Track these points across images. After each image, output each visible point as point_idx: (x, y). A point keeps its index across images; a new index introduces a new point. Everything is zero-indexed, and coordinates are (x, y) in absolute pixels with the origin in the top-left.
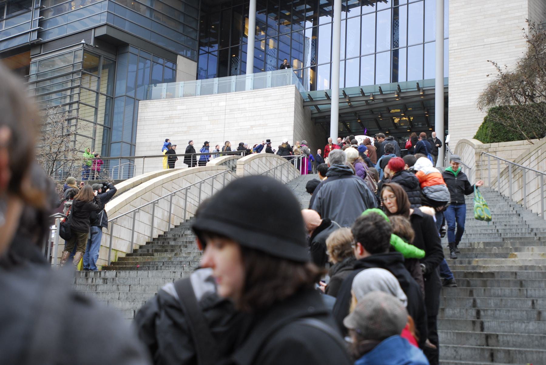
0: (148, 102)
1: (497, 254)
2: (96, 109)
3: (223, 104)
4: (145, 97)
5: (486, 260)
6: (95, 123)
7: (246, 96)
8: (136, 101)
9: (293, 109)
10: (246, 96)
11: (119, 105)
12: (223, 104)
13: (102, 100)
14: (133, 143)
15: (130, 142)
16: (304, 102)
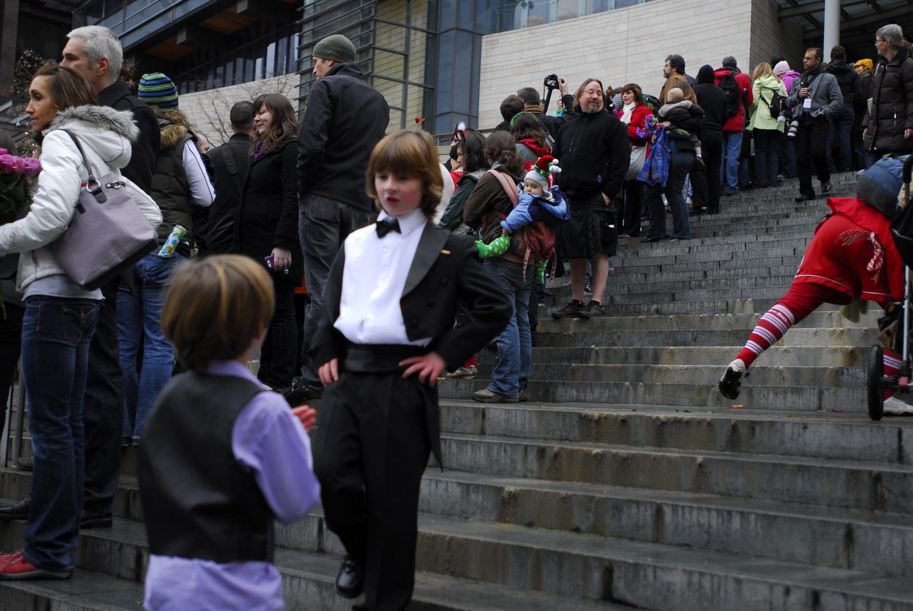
0: (496, 36)
1: (737, 332)
2: (406, 57)
3: (623, 27)
4: (498, 26)
5: (691, 350)
6: (405, 82)
7: (663, 8)
8: (475, 37)
9: (748, 26)
10: (663, 8)
11: (446, 48)
12: (623, 27)
13: (419, 41)
14: (474, 114)
15: (466, 111)
16: (780, 8)
